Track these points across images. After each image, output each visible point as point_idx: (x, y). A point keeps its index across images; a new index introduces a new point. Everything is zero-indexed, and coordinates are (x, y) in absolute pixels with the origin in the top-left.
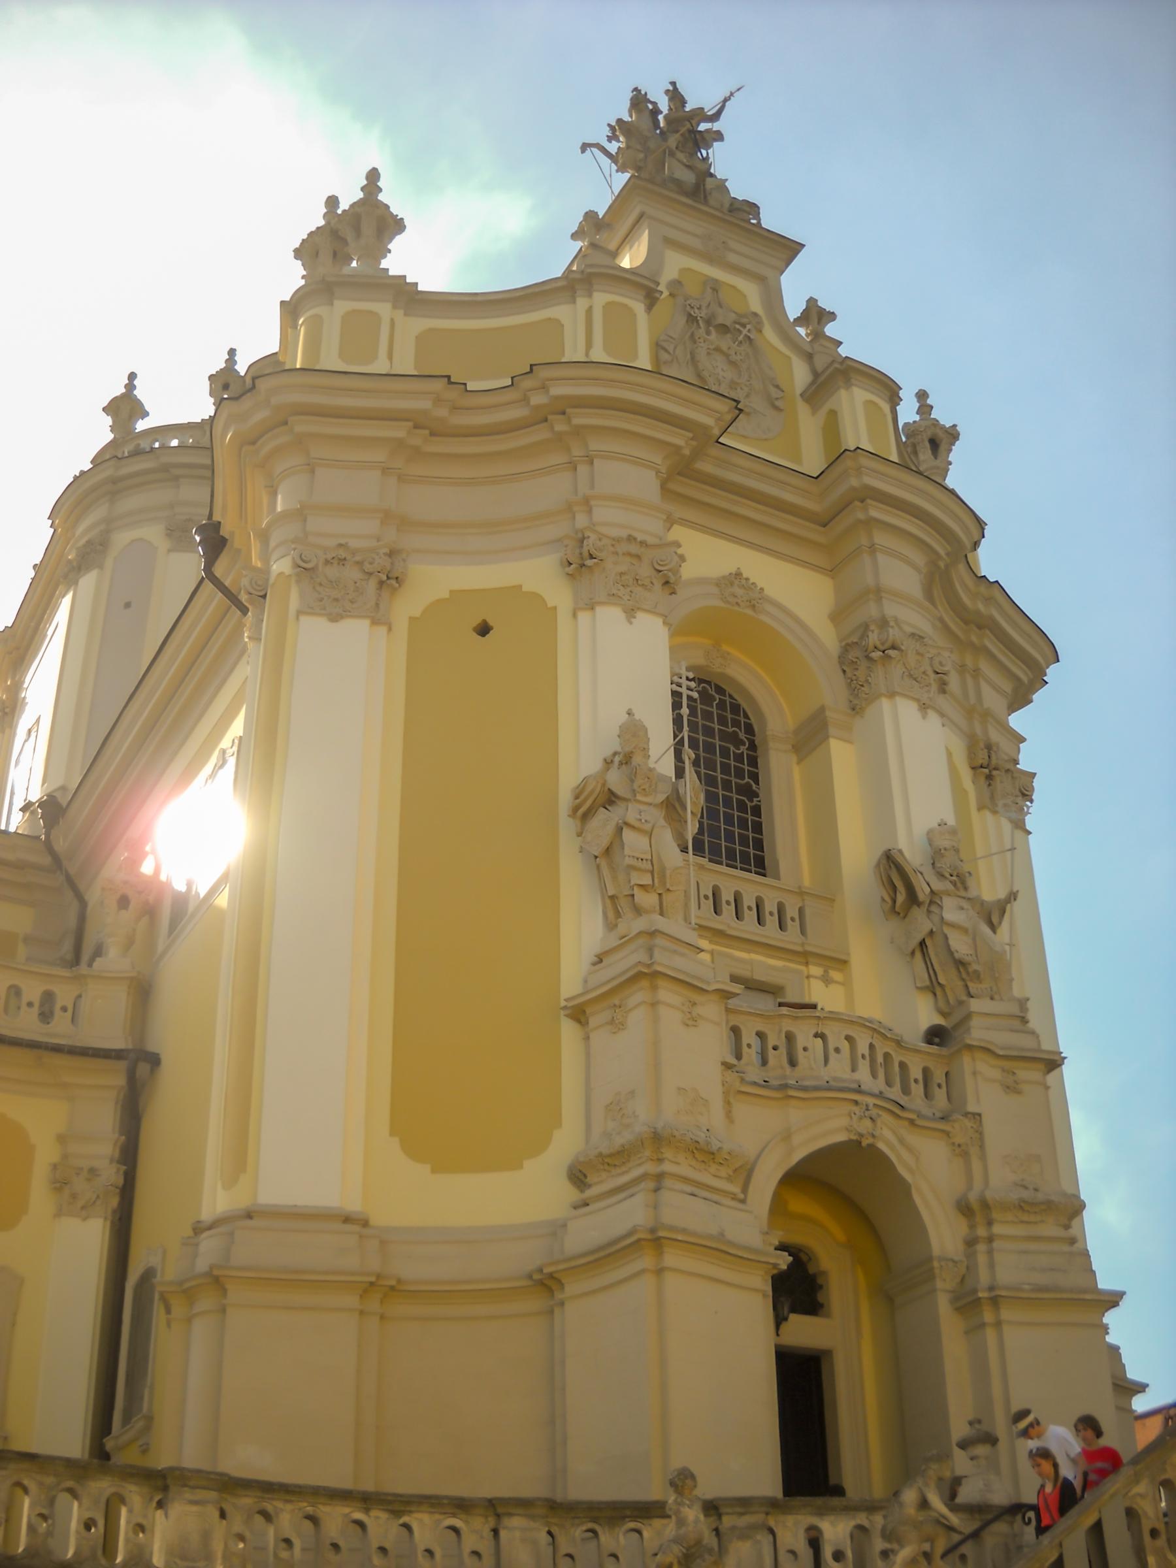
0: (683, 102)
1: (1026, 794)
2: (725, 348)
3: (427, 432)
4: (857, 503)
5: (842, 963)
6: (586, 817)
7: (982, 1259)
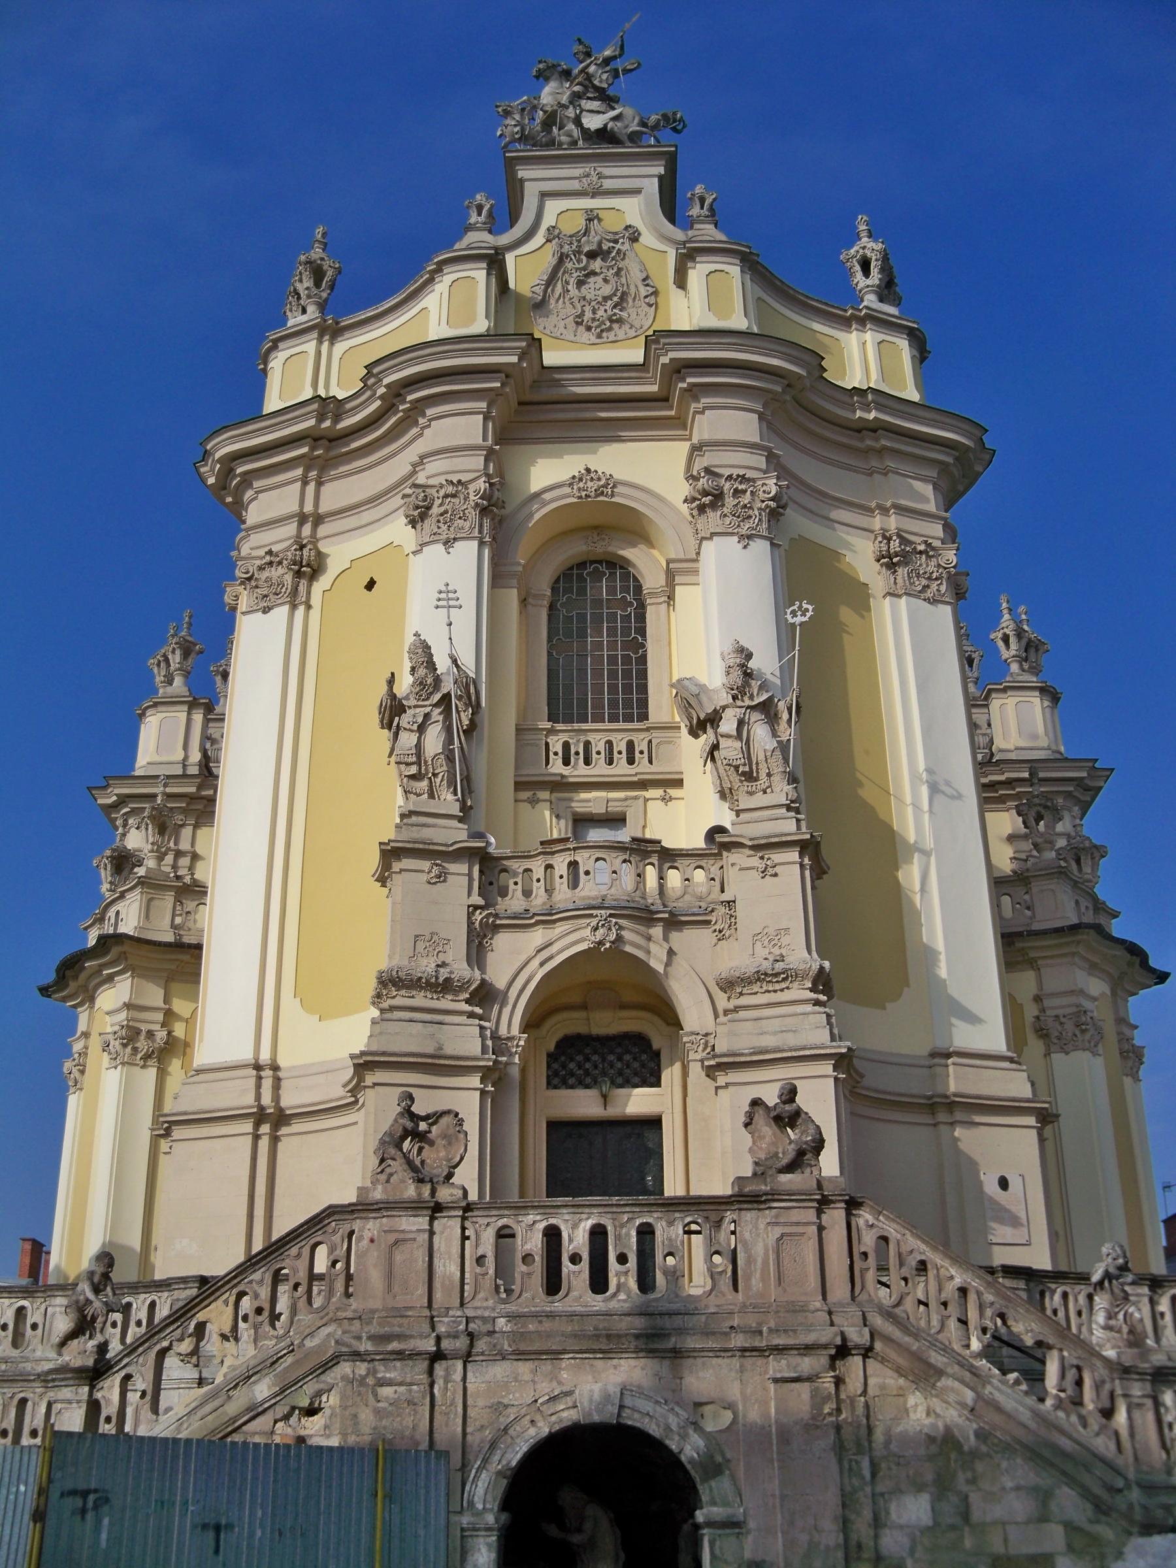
2: (598, 270)
5: (679, 783)
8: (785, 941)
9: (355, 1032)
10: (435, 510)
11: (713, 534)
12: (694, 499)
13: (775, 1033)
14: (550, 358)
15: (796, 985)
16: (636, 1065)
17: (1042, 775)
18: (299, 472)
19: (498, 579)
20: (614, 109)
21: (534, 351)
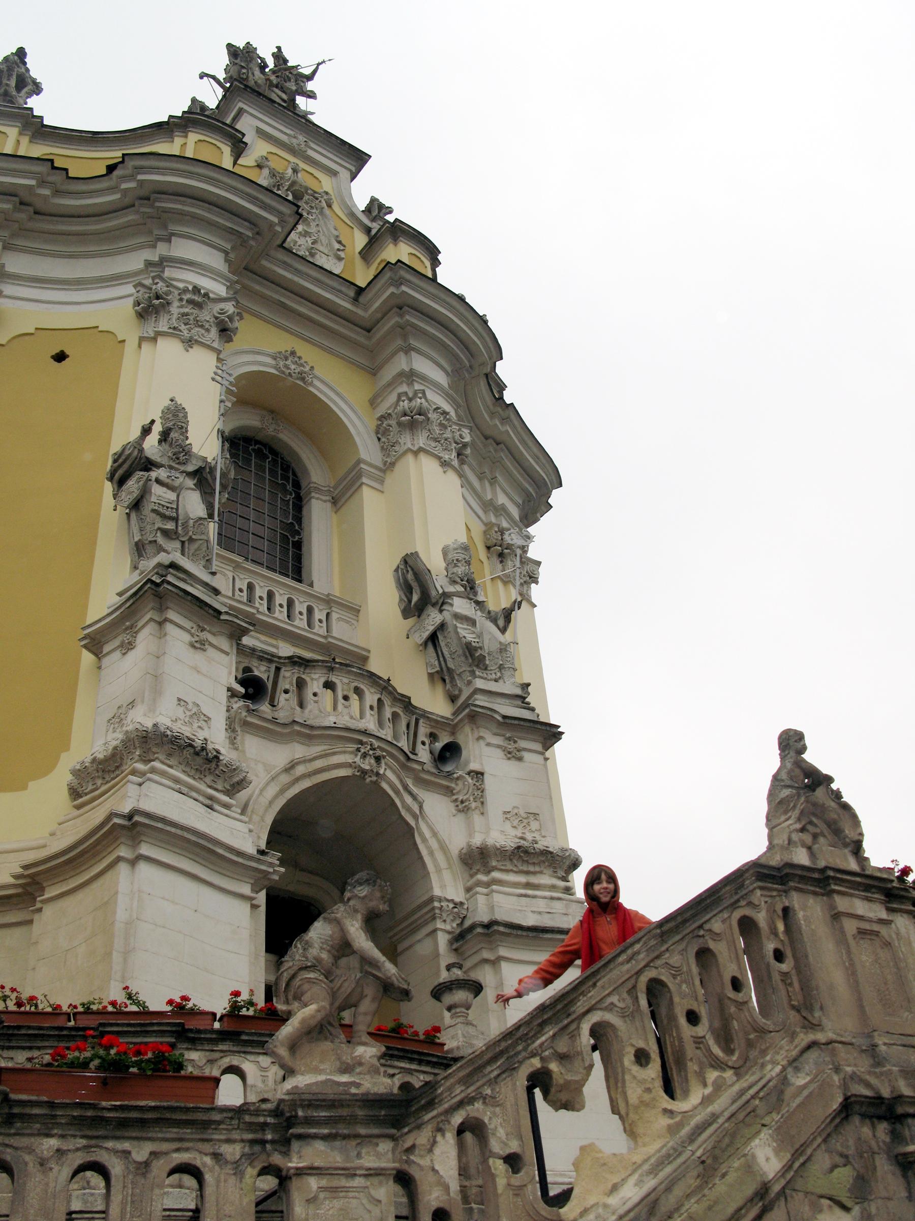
0: (285, 61)
1: (533, 578)
3: (31, 209)
4: (395, 309)
6: (121, 482)
8: (534, 825)
10: (175, 309)
11: (421, 449)
21: (292, 221)
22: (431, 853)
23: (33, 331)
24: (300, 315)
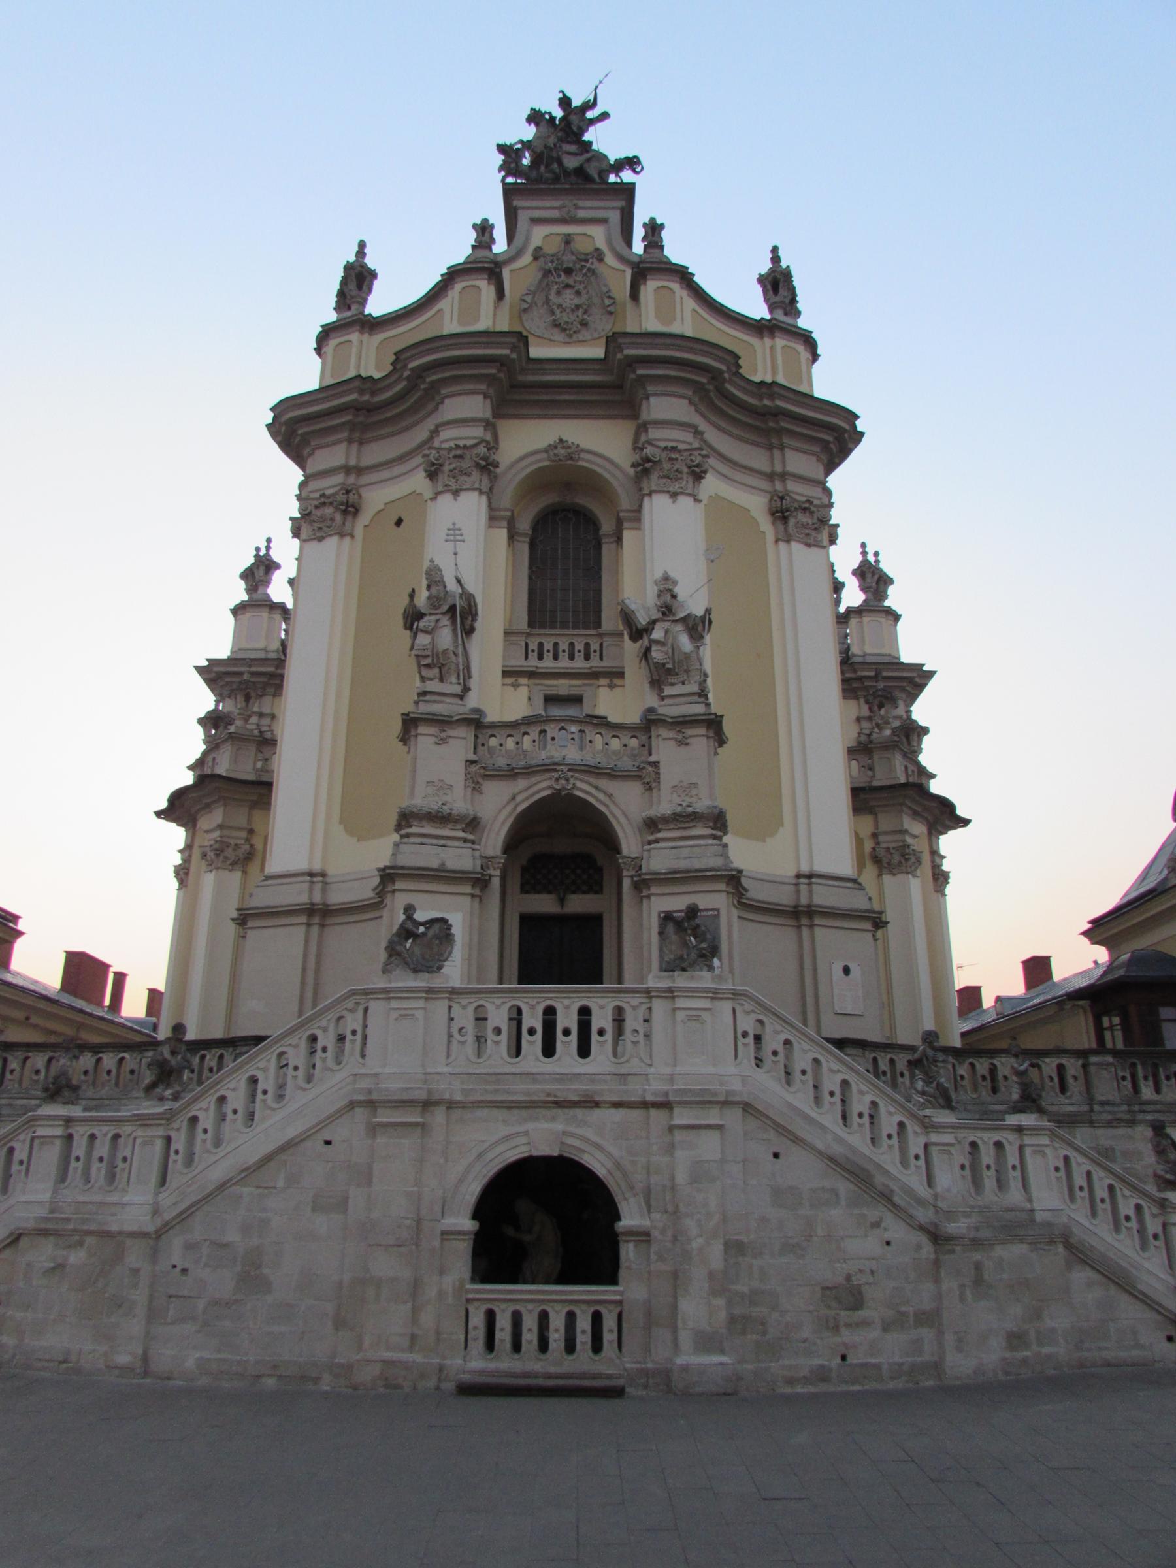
5: (621, 675)
7: (645, 854)
8: (694, 792)
9: (380, 851)
10: (446, 468)
12: (639, 465)
13: (685, 858)
14: (535, 352)
15: (700, 824)
16: (585, 877)
17: (885, 674)
18: (345, 434)
19: (493, 519)
20: (587, 152)
21: (521, 345)
22: (622, 826)
23: (382, 507)
24: (566, 401)
